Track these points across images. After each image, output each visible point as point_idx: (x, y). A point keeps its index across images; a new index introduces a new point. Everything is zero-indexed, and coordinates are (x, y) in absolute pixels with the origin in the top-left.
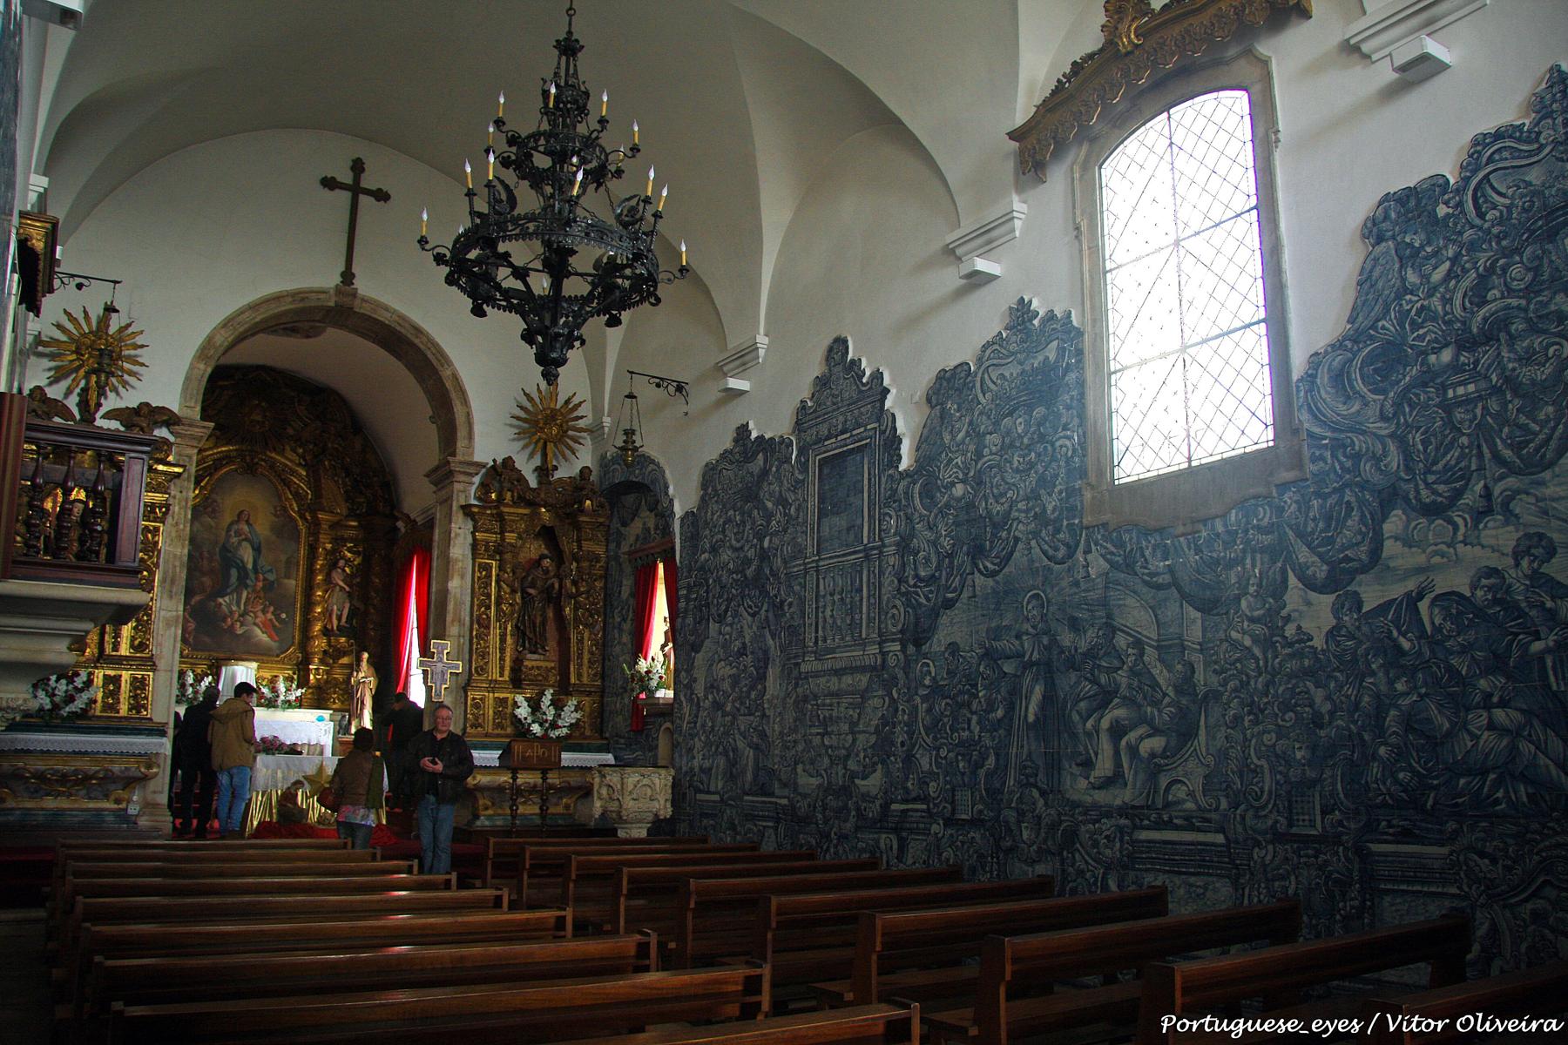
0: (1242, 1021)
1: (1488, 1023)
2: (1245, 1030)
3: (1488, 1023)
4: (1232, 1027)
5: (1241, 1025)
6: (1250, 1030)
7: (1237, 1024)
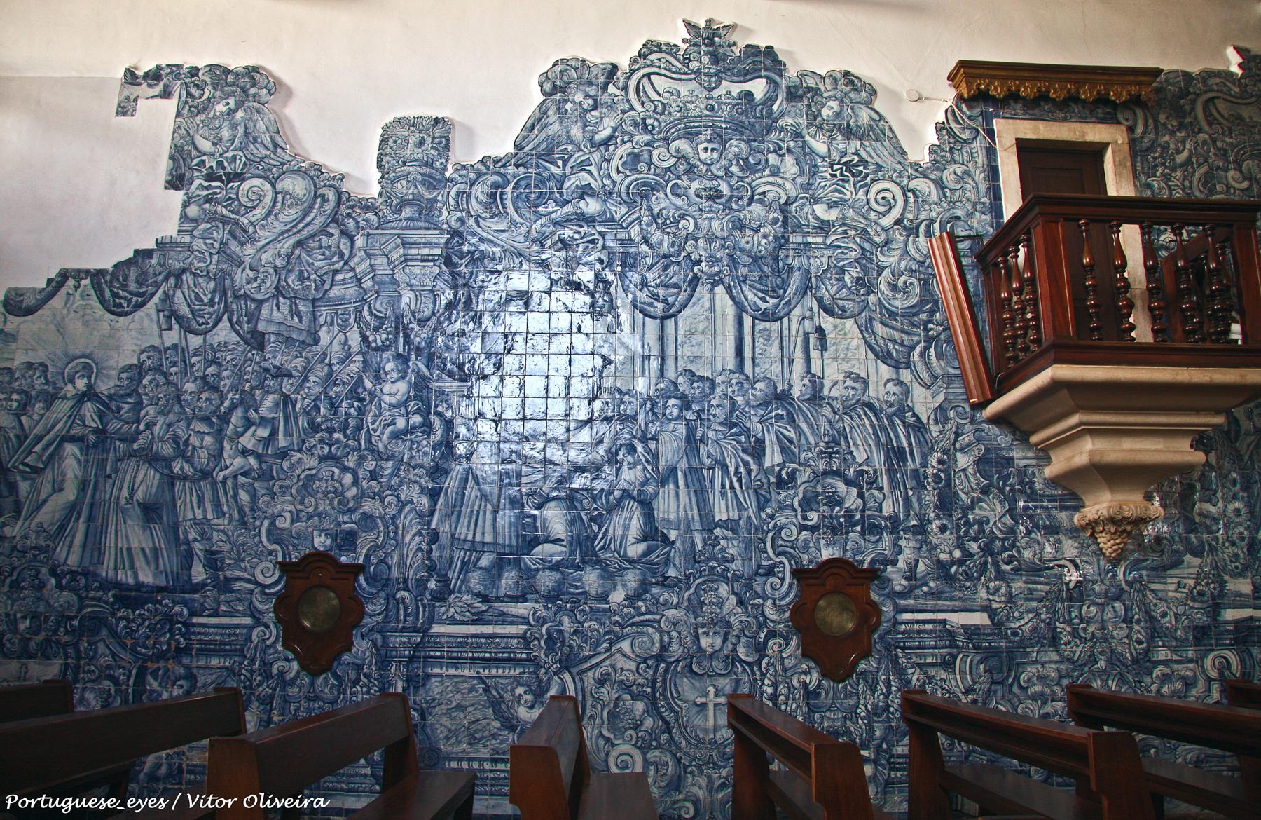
0: (71, 799)
1: (269, 801)
2: (74, 807)
3: (269, 801)
4: (63, 804)
5: (70, 803)
6: (77, 806)
7: (67, 801)
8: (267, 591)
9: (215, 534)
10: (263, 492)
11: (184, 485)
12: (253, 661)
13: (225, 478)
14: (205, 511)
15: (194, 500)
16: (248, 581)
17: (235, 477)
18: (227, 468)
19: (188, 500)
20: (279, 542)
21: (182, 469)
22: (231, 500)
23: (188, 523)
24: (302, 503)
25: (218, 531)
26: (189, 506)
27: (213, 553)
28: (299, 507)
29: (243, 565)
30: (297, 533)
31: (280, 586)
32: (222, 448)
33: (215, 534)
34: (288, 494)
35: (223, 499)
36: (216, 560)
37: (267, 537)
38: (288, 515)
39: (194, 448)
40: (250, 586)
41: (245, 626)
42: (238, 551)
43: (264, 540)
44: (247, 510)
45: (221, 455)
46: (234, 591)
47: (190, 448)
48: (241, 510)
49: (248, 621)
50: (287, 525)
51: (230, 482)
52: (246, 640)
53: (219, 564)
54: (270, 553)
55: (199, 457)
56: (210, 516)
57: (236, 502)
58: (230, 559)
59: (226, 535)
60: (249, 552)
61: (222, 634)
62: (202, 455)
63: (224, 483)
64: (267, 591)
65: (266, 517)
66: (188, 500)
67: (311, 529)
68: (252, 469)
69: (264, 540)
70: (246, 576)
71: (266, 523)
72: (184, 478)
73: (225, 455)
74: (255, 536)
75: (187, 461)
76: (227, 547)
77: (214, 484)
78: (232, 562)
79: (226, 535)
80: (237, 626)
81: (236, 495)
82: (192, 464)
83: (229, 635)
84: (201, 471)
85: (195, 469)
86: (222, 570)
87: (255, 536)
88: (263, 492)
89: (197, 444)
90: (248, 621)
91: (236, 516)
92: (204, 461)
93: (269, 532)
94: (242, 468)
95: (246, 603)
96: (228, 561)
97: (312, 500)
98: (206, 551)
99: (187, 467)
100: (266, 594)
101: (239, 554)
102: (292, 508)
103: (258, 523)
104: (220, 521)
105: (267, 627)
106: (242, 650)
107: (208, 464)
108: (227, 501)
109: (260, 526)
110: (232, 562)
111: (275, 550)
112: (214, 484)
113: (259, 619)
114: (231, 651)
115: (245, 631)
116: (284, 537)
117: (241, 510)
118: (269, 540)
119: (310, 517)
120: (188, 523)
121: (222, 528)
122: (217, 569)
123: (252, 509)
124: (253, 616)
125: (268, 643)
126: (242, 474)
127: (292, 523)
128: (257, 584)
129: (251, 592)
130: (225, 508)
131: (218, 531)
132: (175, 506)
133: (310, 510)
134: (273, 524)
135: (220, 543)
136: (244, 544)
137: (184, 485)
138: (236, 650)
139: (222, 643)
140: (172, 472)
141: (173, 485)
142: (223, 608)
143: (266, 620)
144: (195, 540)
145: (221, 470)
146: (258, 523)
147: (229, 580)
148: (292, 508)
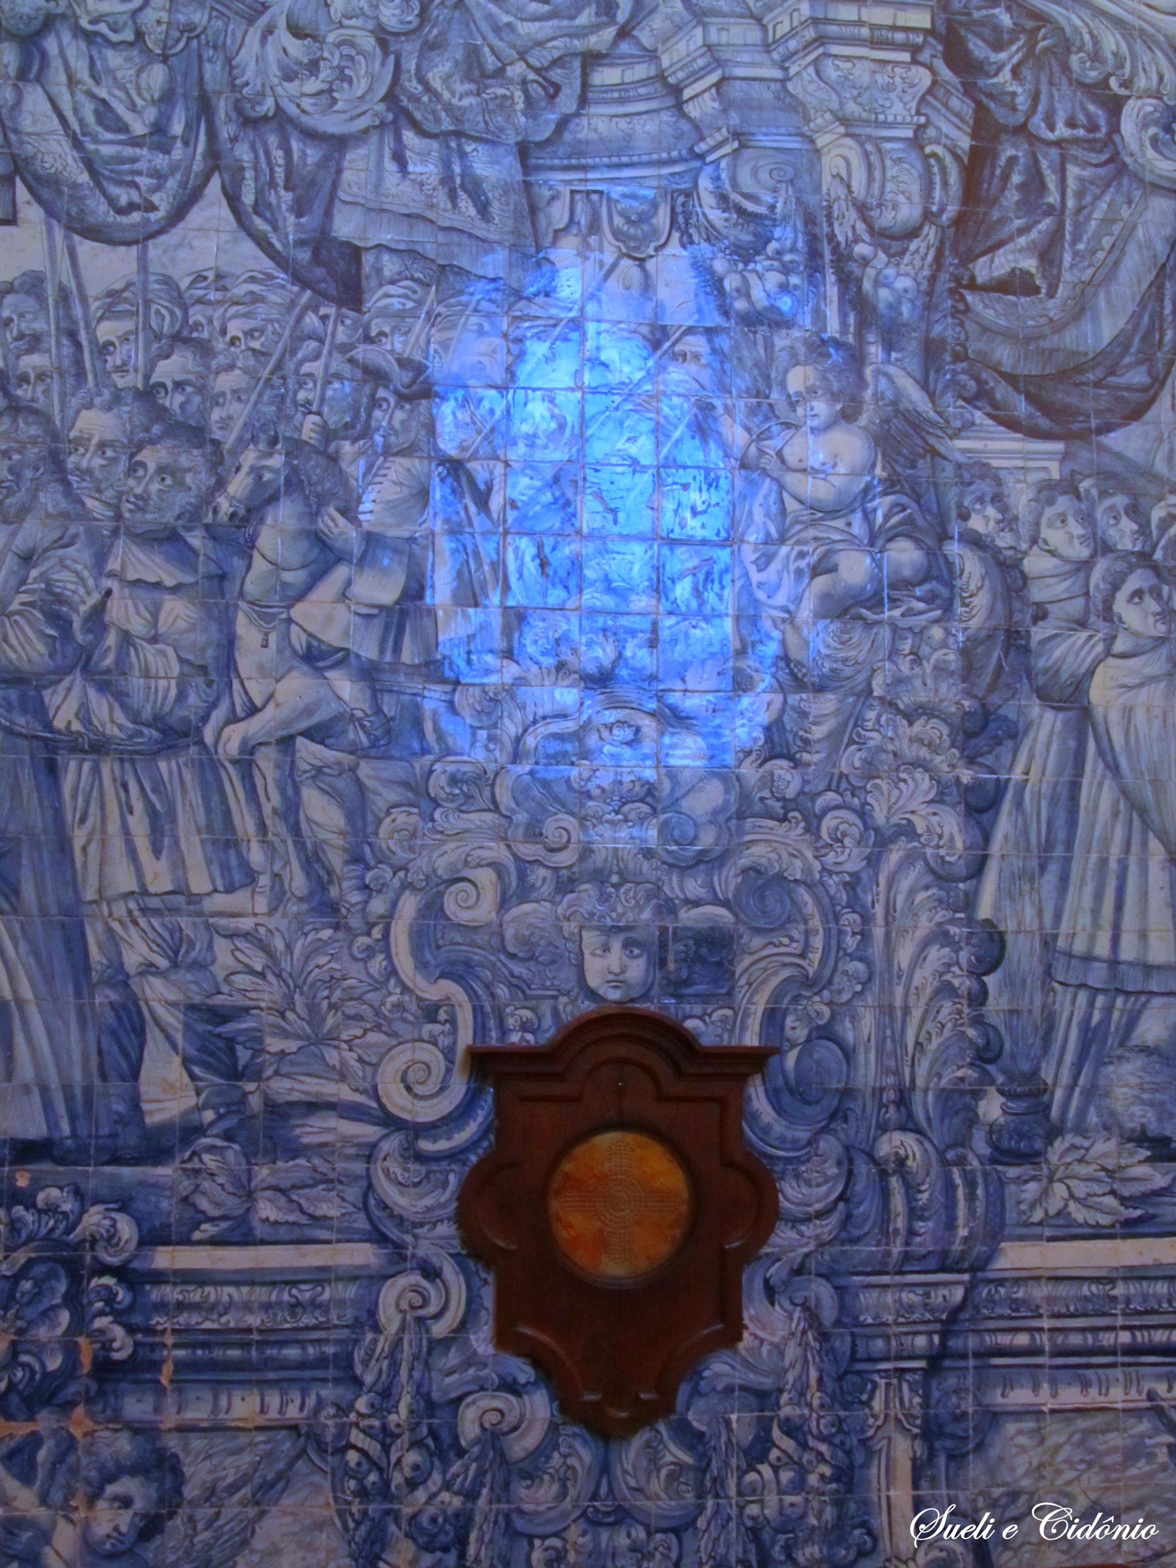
8: (425, 1145)
9: (222, 947)
10: (391, 795)
11: (96, 771)
12: (386, 1395)
13: (249, 749)
14: (179, 864)
15: (139, 824)
16: (353, 1112)
17: (286, 743)
18: (253, 710)
19: (114, 826)
20: (459, 971)
21: (84, 713)
22: (277, 827)
23: (120, 909)
24: (534, 833)
25: (231, 936)
26: (117, 844)
27: (219, 1016)
28: (529, 851)
29: (332, 1057)
30: (526, 942)
31: (470, 1130)
32: (230, 643)
33: (222, 947)
34: (483, 800)
35: (245, 822)
36: (230, 1043)
37: (417, 950)
38: (485, 877)
39: (126, 638)
40: (368, 1131)
41: (352, 1276)
42: (312, 1008)
43: (405, 963)
44: (336, 860)
45: (229, 665)
46: (295, 1151)
47: (111, 639)
48: (312, 860)
49: (363, 1255)
50: (485, 911)
51: (267, 763)
52: (357, 1325)
53: (243, 1055)
54: (430, 1013)
55: (146, 674)
56: (199, 883)
57: (296, 830)
58: (285, 1034)
59: (264, 948)
60: (351, 1008)
61: (267, 1307)
62: (156, 664)
63: (246, 763)
64: (425, 1145)
65: (406, 886)
66: (114, 826)
67: (570, 927)
68: (346, 718)
69: (405, 963)
70: (345, 1093)
71: (409, 906)
72: (98, 747)
73: (245, 663)
74: (370, 952)
75: (104, 687)
76: (270, 993)
77: (209, 767)
78: (291, 1046)
79: (264, 948)
80: (322, 1276)
81: (291, 810)
82: (120, 697)
83: (295, 1307)
84: (158, 721)
85: (135, 716)
86: (257, 1076)
87: (370, 952)
88: (392, 796)
89: (138, 625)
90: (363, 1255)
91: (298, 882)
92: (167, 688)
93: (421, 939)
94: (308, 711)
95: (353, 1193)
96: (274, 1044)
97: (570, 822)
98: (192, 1008)
99: (102, 708)
100: (421, 1158)
101: (314, 1015)
102: (498, 851)
103: (378, 906)
104: (239, 899)
105: (431, 1273)
106: (345, 1362)
107: (181, 696)
108: (262, 827)
109: (387, 919)
110: (291, 1046)
111: (447, 1001)
112: (209, 767)
113: (399, 1246)
114: (303, 1365)
115: (350, 1292)
116: (478, 955)
117: (312, 860)
118: (422, 965)
119: (566, 885)
120: (120, 909)
121: (246, 923)
122: (235, 1074)
123: (356, 859)
124: (380, 1238)
125: (440, 1329)
126: (307, 734)
127: (503, 904)
128: (390, 1122)
129: (369, 1152)
130: (256, 855)
131: (231, 936)
132: (64, 845)
133: (565, 858)
134: (433, 909)
135: (242, 981)
136: (332, 981)
137: (96, 771)
138: (322, 1362)
139: (270, 1337)
140: (48, 726)
141: (52, 770)
142: (267, 1209)
143: (425, 1249)
144: (149, 969)
145: (233, 719)
146: (378, 906)
147: (278, 1111)
148: (498, 851)
